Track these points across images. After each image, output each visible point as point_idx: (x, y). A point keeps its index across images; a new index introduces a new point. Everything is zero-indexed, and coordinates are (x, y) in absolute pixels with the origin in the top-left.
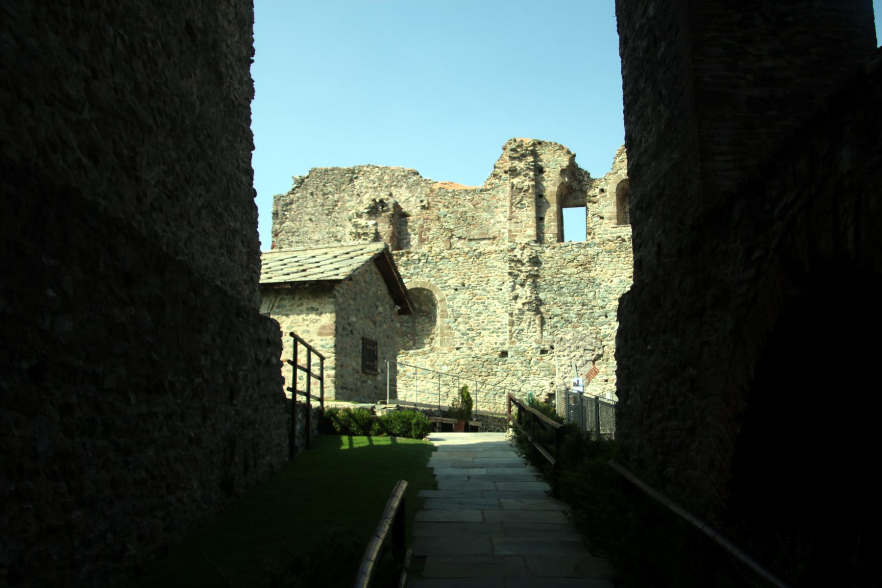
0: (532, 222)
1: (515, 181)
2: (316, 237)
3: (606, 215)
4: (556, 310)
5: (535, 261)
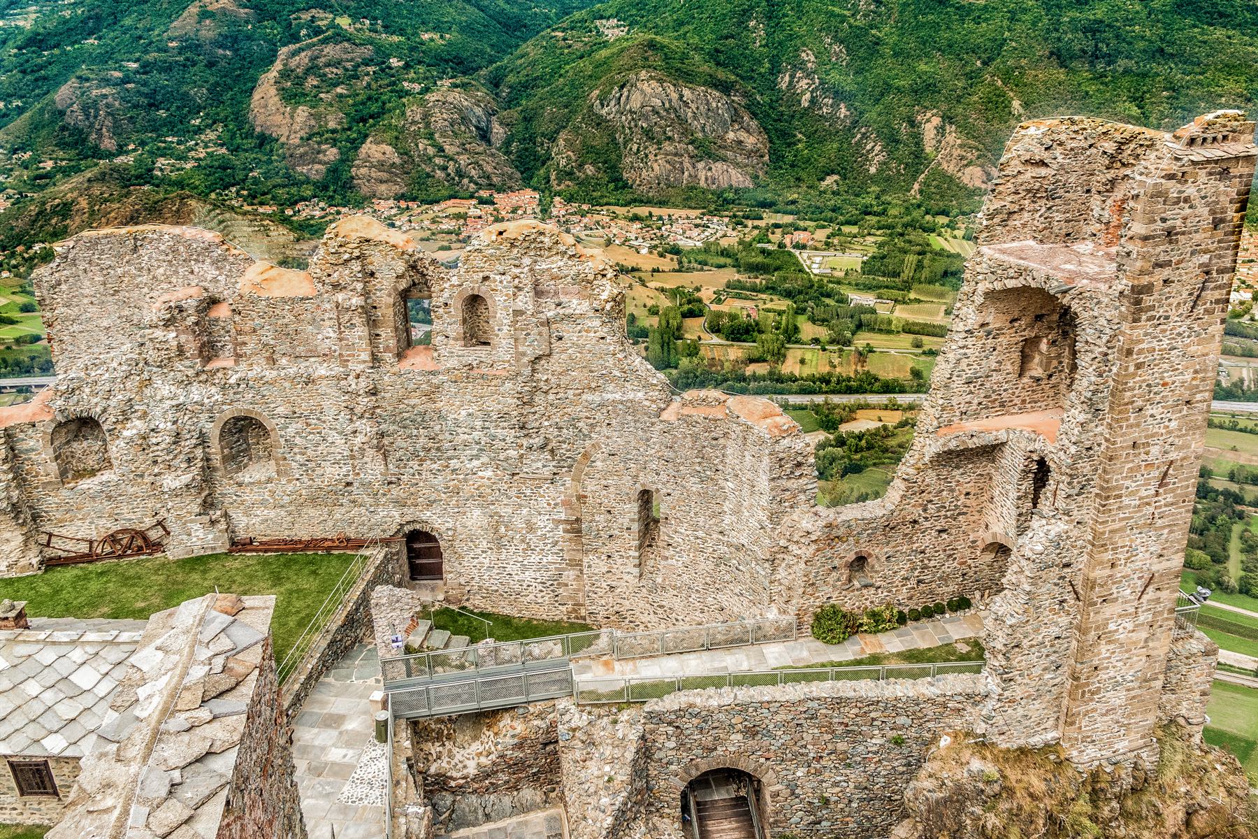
0: (364, 344)
1: (340, 297)
2: (105, 324)
3: (452, 334)
4: (400, 443)
5: (374, 392)
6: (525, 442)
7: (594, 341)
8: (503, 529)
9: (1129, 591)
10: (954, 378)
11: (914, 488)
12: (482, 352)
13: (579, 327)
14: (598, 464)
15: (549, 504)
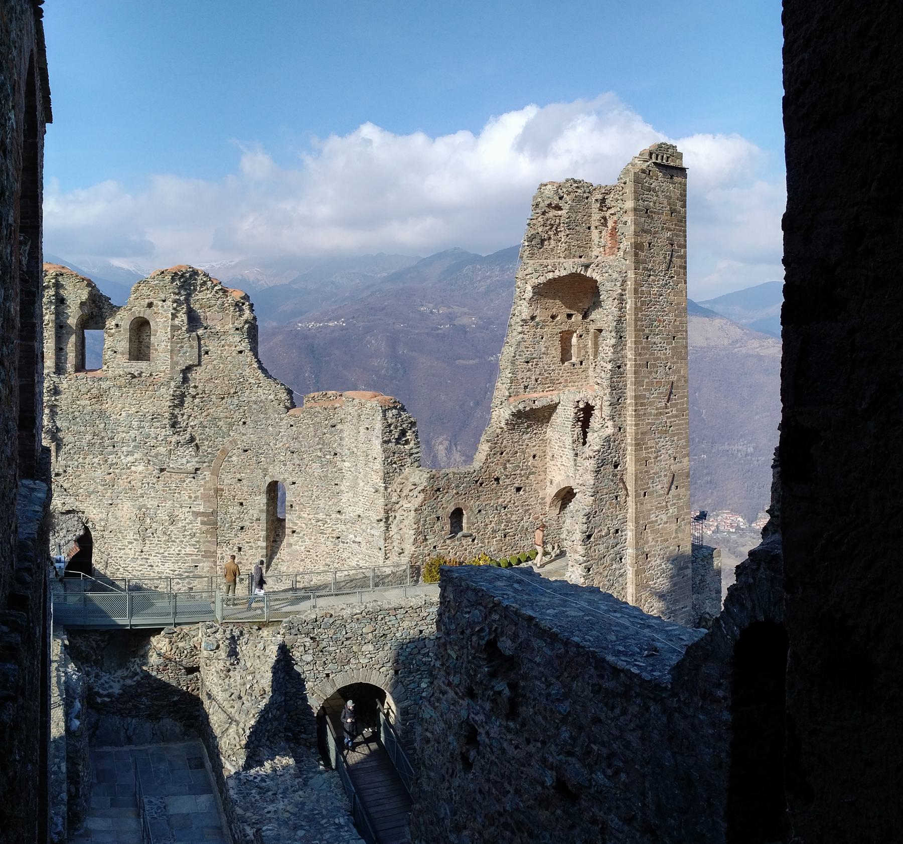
3: (120, 349)
6: (174, 439)
7: (234, 354)
8: (148, 521)
9: (659, 487)
10: (517, 357)
11: (497, 450)
12: (143, 365)
13: (223, 342)
14: (234, 458)
15: (190, 497)
